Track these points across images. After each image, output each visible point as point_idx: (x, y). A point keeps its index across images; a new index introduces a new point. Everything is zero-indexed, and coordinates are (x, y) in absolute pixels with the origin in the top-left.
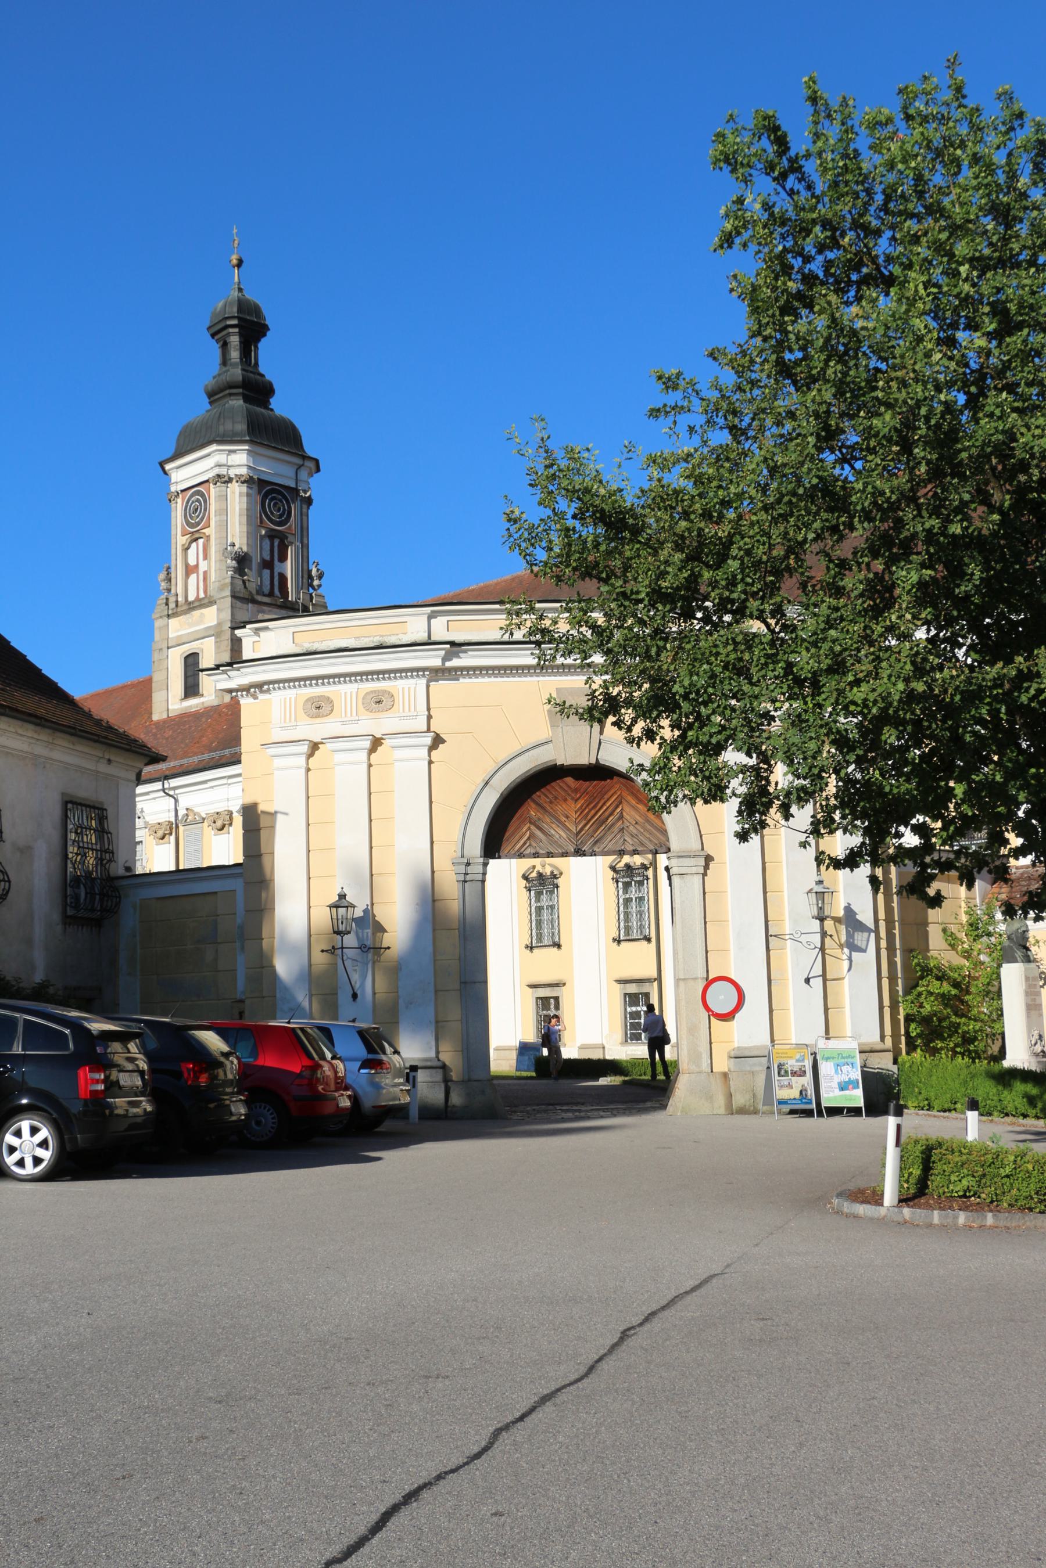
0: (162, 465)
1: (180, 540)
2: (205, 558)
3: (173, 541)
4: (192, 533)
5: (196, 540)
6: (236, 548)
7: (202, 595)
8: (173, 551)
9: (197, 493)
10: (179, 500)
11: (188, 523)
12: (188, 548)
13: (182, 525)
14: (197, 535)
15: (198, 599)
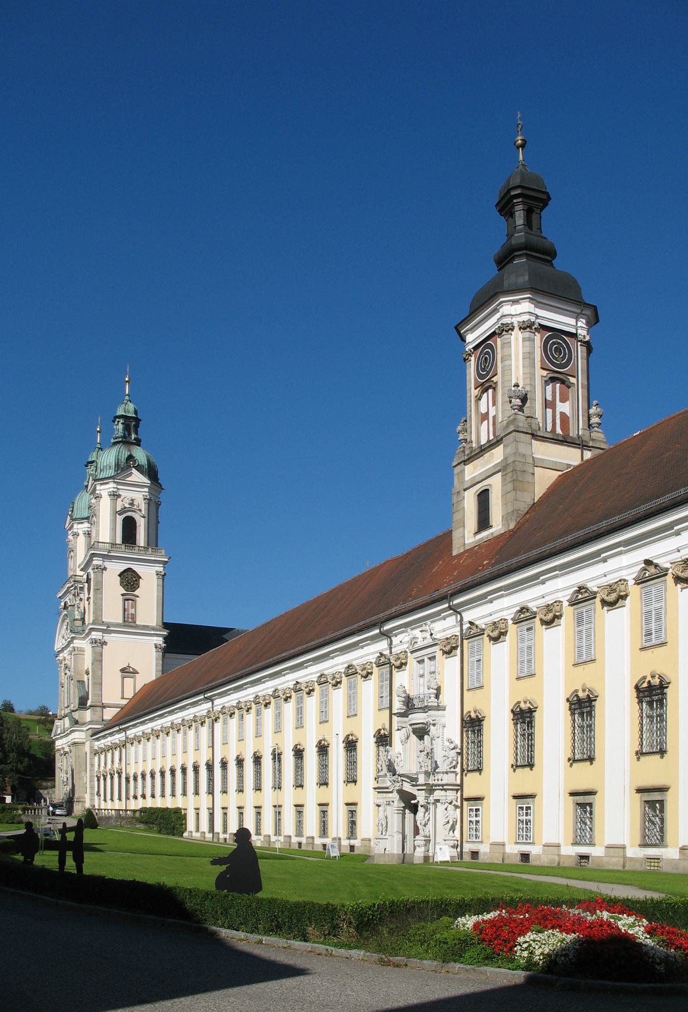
0: (457, 329)
1: (474, 392)
2: (494, 404)
3: (468, 395)
4: (482, 384)
5: (486, 390)
6: (520, 388)
7: (491, 437)
8: (468, 399)
9: (486, 344)
10: (473, 358)
11: (480, 376)
12: (480, 399)
13: (475, 379)
14: (487, 385)
15: (489, 441)
